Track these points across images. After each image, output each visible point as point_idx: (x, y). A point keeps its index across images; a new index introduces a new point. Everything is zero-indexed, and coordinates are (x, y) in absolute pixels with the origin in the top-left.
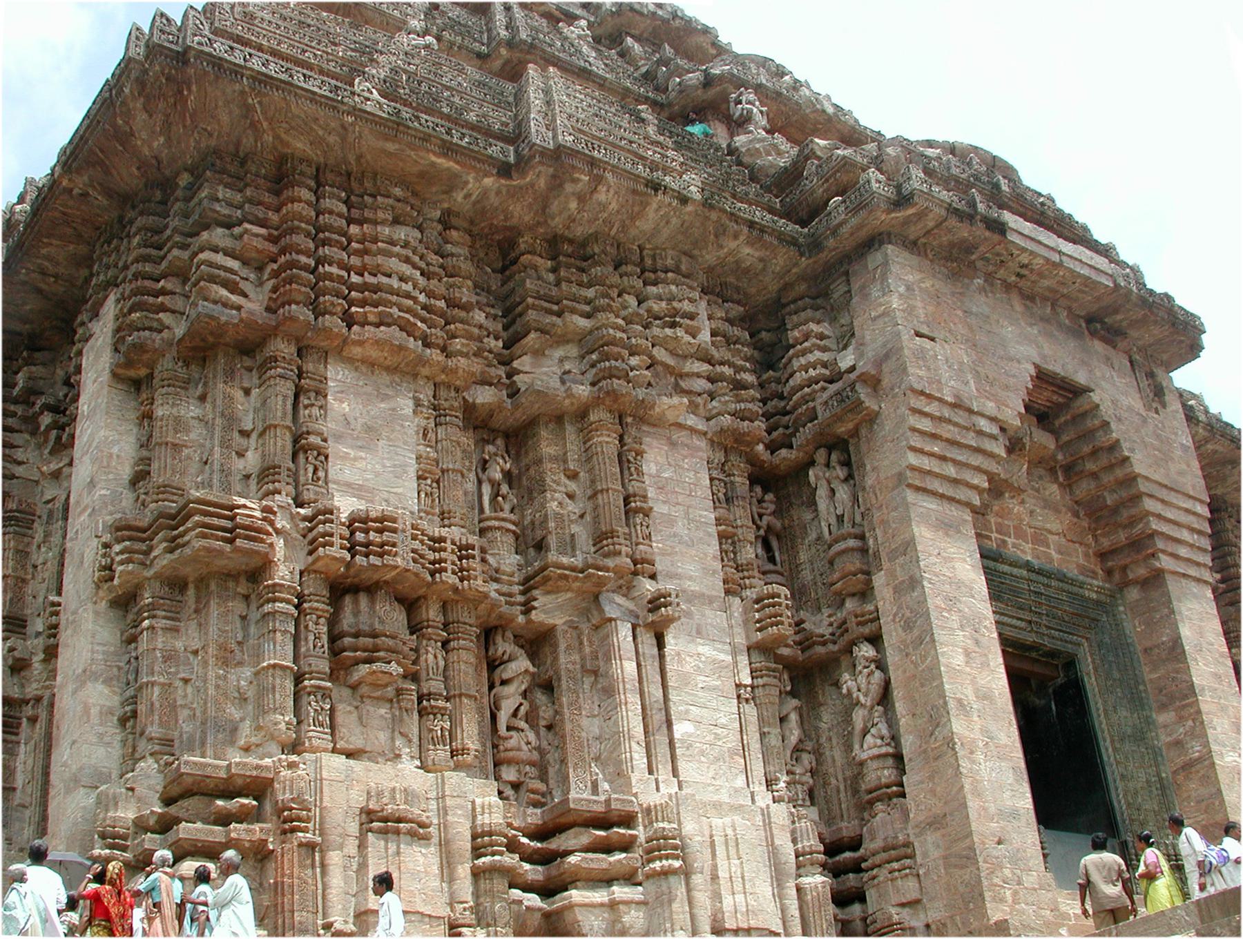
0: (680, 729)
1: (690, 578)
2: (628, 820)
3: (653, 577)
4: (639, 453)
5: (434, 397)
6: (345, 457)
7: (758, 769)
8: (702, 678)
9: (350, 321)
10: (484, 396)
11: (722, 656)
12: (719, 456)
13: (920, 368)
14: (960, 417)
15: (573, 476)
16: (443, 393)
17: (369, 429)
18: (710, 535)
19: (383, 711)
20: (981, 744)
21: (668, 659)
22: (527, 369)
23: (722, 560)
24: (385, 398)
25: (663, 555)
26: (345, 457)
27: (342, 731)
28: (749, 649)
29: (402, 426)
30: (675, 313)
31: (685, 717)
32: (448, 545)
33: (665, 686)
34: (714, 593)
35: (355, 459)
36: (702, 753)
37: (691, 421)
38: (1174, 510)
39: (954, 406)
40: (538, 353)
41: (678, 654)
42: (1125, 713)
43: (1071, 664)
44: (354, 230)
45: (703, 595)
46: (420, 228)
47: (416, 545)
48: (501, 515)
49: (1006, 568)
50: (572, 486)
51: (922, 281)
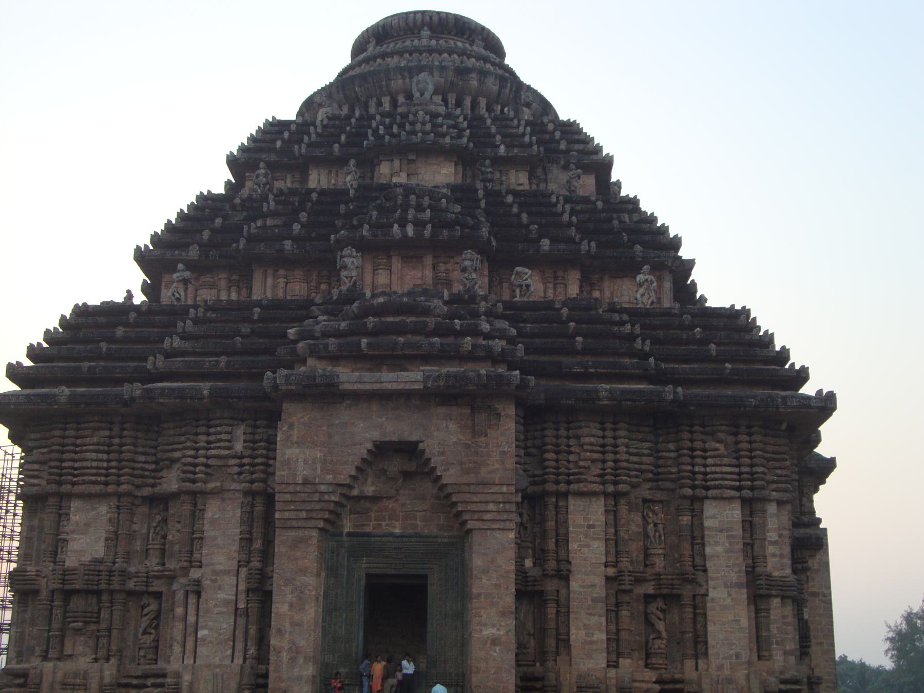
0: (201, 634)
1: (220, 564)
2: (164, 676)
3: (201, 567)
4: (204, 510)
5: (119, 502)
6: (75, 540)
7: (240, 646)
8: (218, 609)
9: (74, 484)
10: (146, 492)
11: (230, 597)
12: (250, 499)
13: (284, 470)
14: (309, 489)
15: (179, 522)
16: (122, 500)
17: (87, 525)
18: (234, 540)
19: (82, 638)
20: (286, 648)
21: (200, 604)
22: (165, 476)
23: (239, 551)
24: (94, 509)
25: (206, 555)
26: (75, 540)
27: (65, 649)
28: (248, 591)
29: (101, 520)
30: (220, 441)
31: (205, 627)
32: (104, 573)
33: (197, 615)
34: (232, 568)
35: (79, 539)
36: (211, 642)
37: (235, 486)
38: (479, 496)
39: (303, 484)
40: (169, 467)
41: (206, 600)
42: (674, 538)
43: (425, 577)
44: (79, 441)
45: (225, 570)
46: (111, 430)
47: (86, 577)
48: (154, 542)
49: (377, 539)
50: (179, 526)
51: (301, 418)
